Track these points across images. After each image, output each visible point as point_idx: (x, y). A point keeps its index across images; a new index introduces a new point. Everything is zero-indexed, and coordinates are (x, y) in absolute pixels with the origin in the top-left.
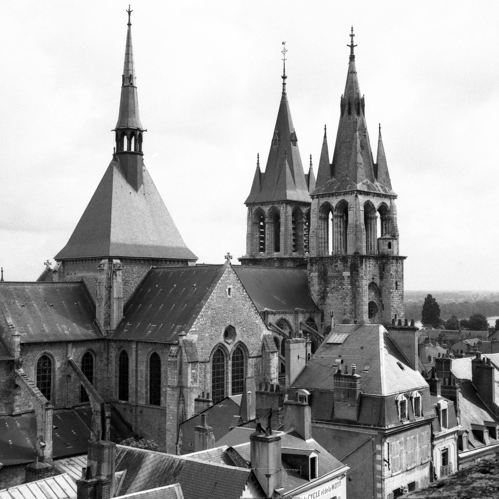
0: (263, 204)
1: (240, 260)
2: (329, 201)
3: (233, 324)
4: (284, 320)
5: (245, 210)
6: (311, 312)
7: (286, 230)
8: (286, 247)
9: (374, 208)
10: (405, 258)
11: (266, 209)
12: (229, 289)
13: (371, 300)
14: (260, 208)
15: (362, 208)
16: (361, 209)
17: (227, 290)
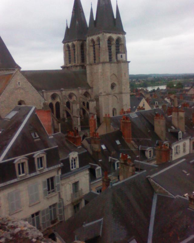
0: (68, 42)
1: (62, 67)
2: (93, 38)
3: (22, 99)
4: (73, 93)
5: (63, 45)
6: (86, 89)
7: (77, 53)
8: (78, 60)
9: (113, 40)
10: (129, 62)
11: (70, 44)
12: (19, 83)
13: (113, 82)
14: (68, 44)
15: (106, 40)
16: (106, 40)
17: (18, 83)
